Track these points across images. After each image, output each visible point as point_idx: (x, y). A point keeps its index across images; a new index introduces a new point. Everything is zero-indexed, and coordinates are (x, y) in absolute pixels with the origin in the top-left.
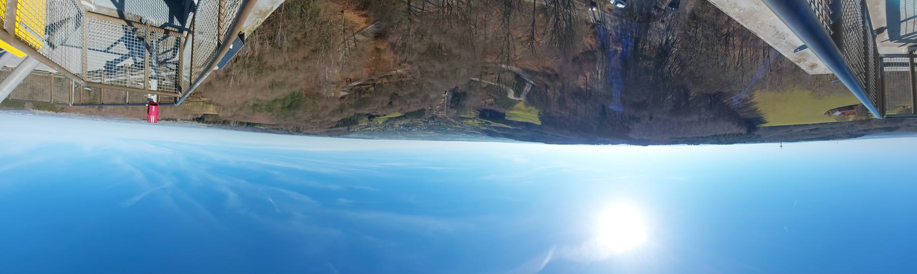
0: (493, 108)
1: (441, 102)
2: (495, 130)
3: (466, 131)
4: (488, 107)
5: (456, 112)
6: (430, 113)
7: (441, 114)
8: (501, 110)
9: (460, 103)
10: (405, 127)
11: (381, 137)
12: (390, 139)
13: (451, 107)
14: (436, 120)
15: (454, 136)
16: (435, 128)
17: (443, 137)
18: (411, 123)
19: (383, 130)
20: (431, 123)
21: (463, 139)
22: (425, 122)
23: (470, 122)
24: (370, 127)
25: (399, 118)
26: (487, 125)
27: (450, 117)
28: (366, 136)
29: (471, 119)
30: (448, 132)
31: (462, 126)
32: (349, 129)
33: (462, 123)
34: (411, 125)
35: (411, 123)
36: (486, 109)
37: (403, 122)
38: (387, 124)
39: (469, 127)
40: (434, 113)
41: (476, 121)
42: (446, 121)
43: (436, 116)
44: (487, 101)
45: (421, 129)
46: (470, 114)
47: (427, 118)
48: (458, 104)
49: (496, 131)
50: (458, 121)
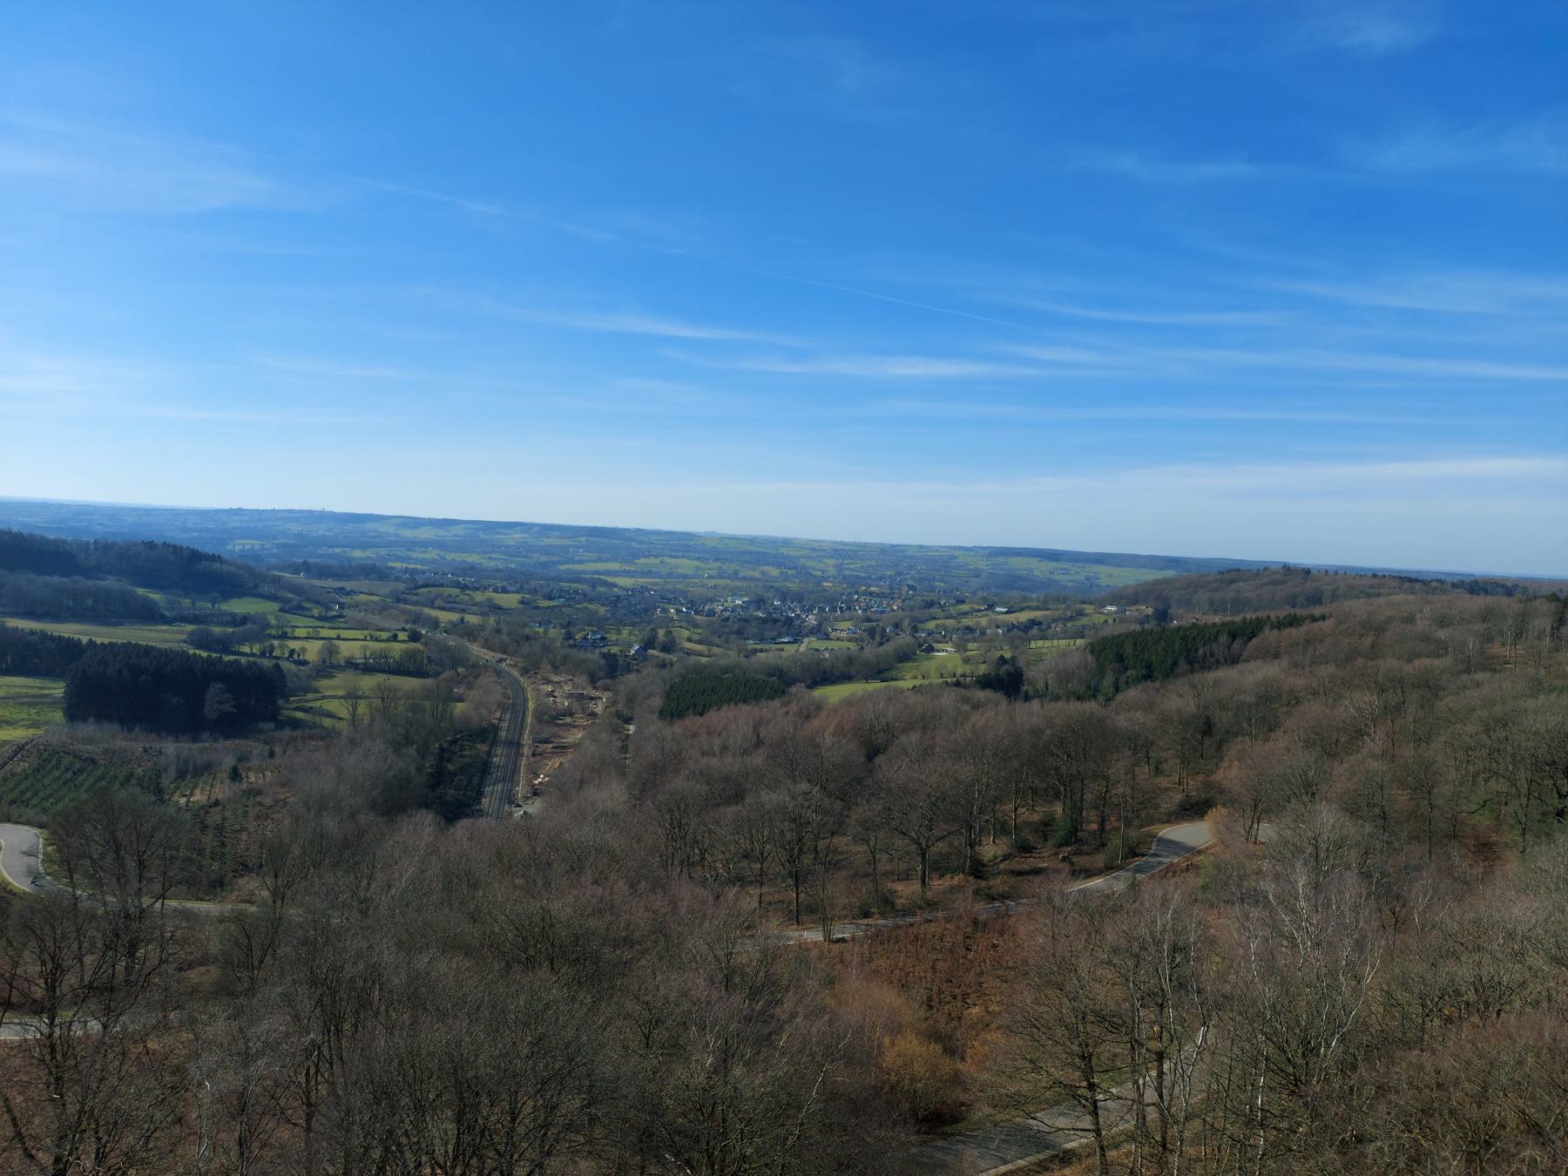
0: (172, 748)
1: (554, 763)
2: (156, 596)
3: (386, 588)
4: (224, 751)
5: (459, 708)
6: (631, 700)
7: (561, 691)
8: (100, 738)
9: (429, 765)
10: (789, 621)
11: (941, 562)
12: (885, 551)
13: (487, 733)
14: (594, 656)
15: (472, 558)
16: (602, 610)
17: (546, 550)
18: (751, 644)
19: (930, 604)
20: (627, 640)
21: (408, 534)
22: (667, 648)
23: (351, 648)
24: (1011, 627)
25: (825, 676)
26: (217, 630)
27: (498, 673)
28: (1041, 569)
29: (351, 665)
30: (514, 579)
31: (417, 619)
32: (1162, 616)
33: (415, 637)
34: (752, 629)
35: (751, 644)
36: (227, 737)
37: (803, 648)
38: (905, 639)
39: (359, 615)
40: (605, 696)
41: (313, 651)
42: (525, 648)
43: (593, 681)
44: (222, 790)
45: (692, 604)
46: (353, 696)
47: (650, 670)
48: (444, 755)
49: (140, 591)
50: (447, 649)
